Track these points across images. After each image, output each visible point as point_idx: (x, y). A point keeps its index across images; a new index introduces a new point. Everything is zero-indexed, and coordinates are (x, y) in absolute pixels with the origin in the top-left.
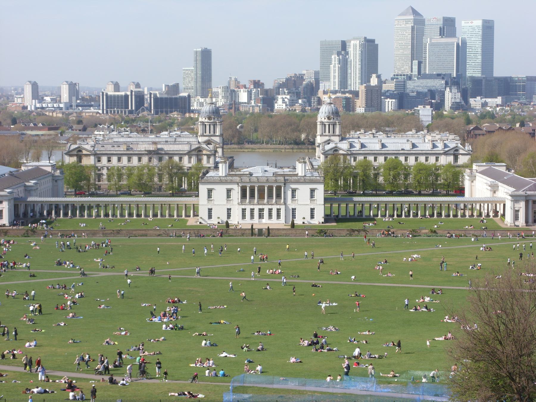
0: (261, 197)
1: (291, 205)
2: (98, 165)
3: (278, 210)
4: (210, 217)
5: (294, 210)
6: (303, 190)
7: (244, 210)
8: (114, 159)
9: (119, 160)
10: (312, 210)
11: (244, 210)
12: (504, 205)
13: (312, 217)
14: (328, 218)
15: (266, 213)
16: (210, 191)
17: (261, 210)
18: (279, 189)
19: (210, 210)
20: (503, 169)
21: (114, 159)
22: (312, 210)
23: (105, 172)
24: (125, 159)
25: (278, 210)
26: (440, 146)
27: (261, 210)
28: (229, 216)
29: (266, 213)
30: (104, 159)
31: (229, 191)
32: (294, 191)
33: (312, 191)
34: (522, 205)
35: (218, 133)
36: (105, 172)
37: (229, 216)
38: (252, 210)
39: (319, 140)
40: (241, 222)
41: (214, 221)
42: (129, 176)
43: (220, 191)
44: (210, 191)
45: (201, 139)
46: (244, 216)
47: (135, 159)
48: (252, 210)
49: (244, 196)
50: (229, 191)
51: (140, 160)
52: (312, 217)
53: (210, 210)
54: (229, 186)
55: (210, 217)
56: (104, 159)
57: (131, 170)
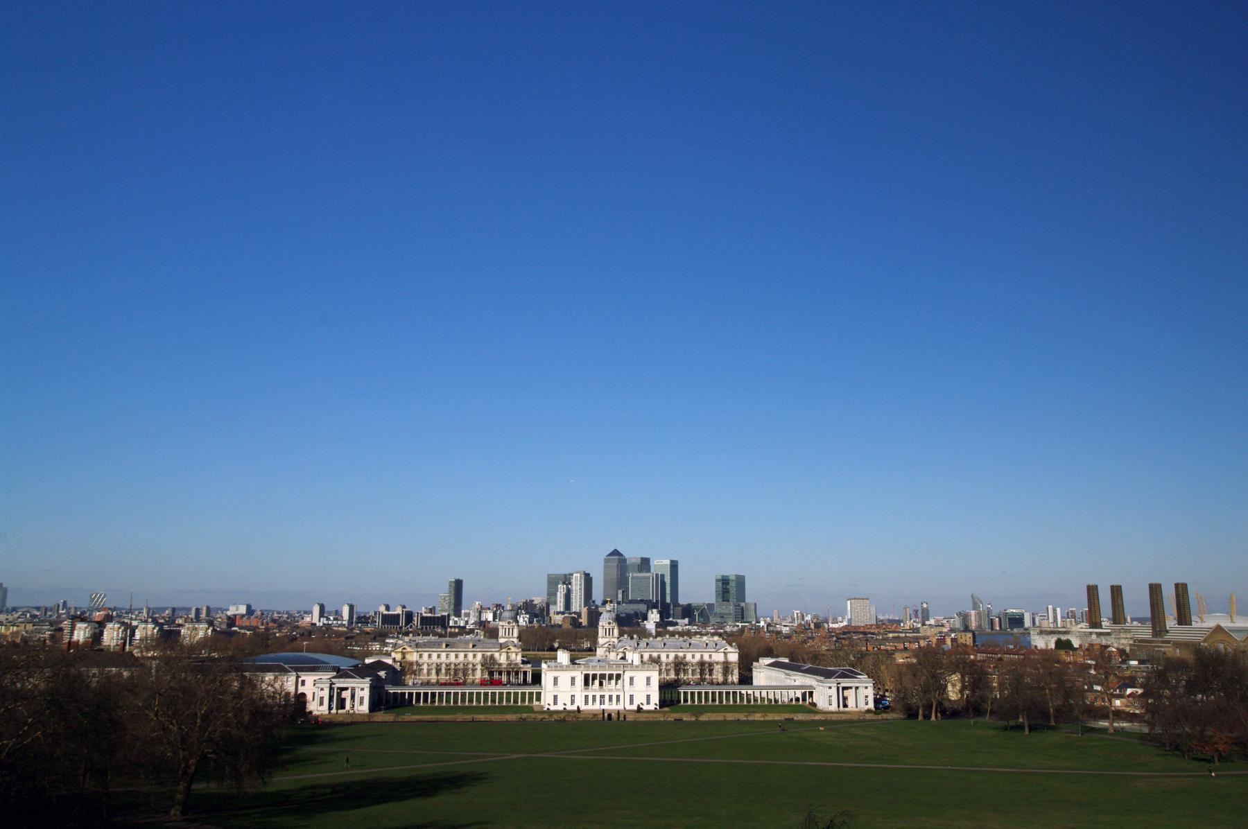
0: (601, 684)
1: (629, 690)
2: (421, 661)
3: (618, 697)
4: (555, 703)
5: (632, 697)
6: (640, 677)
7: (587, 697)
8: (435, 655)
9: (439, 656)
10: (648, 697)
11: (587, 697)
12: (811, 694)
13: (648, 703)
14: (663, 703)
15: (607, 699)
16: (556, 679)
17: (602, 697)
18: (618, 677)
19: (555, 697)
20: (786, 660)
21: (435, 655)
22: (648, 697)
23: (425, 667)
24: (443, 655)
25: (618, 697)
26: (712, 644)
27: (602, 697)
28: (573, 702)
29: (607, 699)
30: (426, 655)
31: (573, 679)
32: (632, 679)
33: (648, 679)
34: (834, 690)
35: (516, 634)
36: (425, 667)
37: (573, 702)
38: (594, 697)
39: (601, 641)
40: (583, 707)
41: (560, 707)
42: (448, 670)
43: (565, 677)
44: (556, 679)
45: (501, 641)
46: (586, 703)
47: (452, 655)
48: (594, 697)
49: (586, 683)
50: (573, 679)
51: (457, 656)
52: (648, 703)
53: (555, 697)
54: (574, 674)
55: (555, 703)
56: (426, 655)
57: (448, 665)
